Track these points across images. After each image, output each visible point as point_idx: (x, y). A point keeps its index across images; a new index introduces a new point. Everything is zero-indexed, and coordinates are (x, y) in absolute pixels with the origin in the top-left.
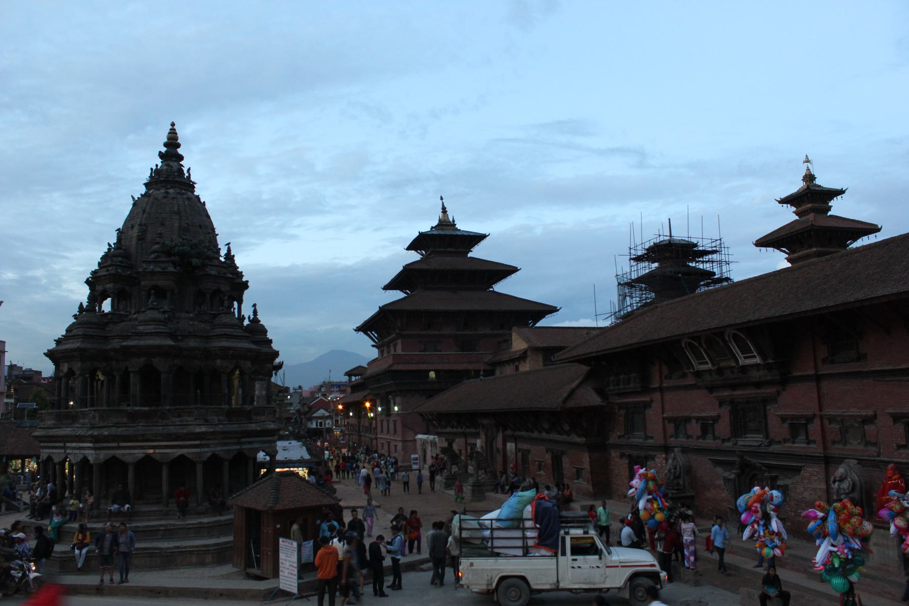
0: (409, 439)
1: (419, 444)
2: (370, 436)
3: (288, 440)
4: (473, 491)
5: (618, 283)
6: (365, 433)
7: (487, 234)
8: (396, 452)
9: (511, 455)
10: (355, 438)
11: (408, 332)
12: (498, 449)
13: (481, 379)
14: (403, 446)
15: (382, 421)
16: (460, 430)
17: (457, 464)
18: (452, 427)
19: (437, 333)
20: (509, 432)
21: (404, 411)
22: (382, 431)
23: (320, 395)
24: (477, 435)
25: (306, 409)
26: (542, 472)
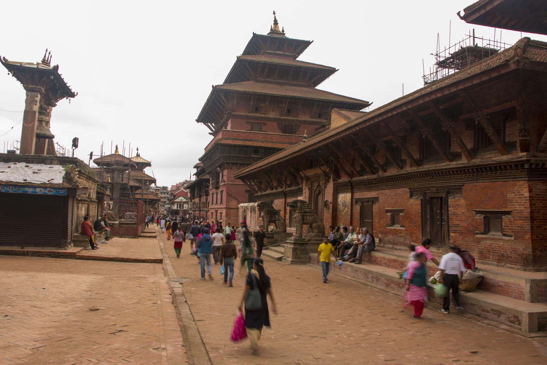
0: (232, 207)
1: (241, 211)
2: (206, 209)
3: (51, 164)
4: (294, 250)
5: (425, 82)
6: (203, 208)
7: (311, 41)
8: (221, 219)
9: (344, 211)
10: (197, 212)
11: (237, 113)
12: (326, 204)
13: (304, 142)
14: (226, 212)
15: (213, 194)
16: (280, 190)
17: (274, 222)
18: (272, 189)
19: (263, 116)
20: (344, 179)
21: (230, 182)
22: (212, 204)
23: (182, 188)
24: (299, 192)
25: (173, 197)
26: (397, 227)
